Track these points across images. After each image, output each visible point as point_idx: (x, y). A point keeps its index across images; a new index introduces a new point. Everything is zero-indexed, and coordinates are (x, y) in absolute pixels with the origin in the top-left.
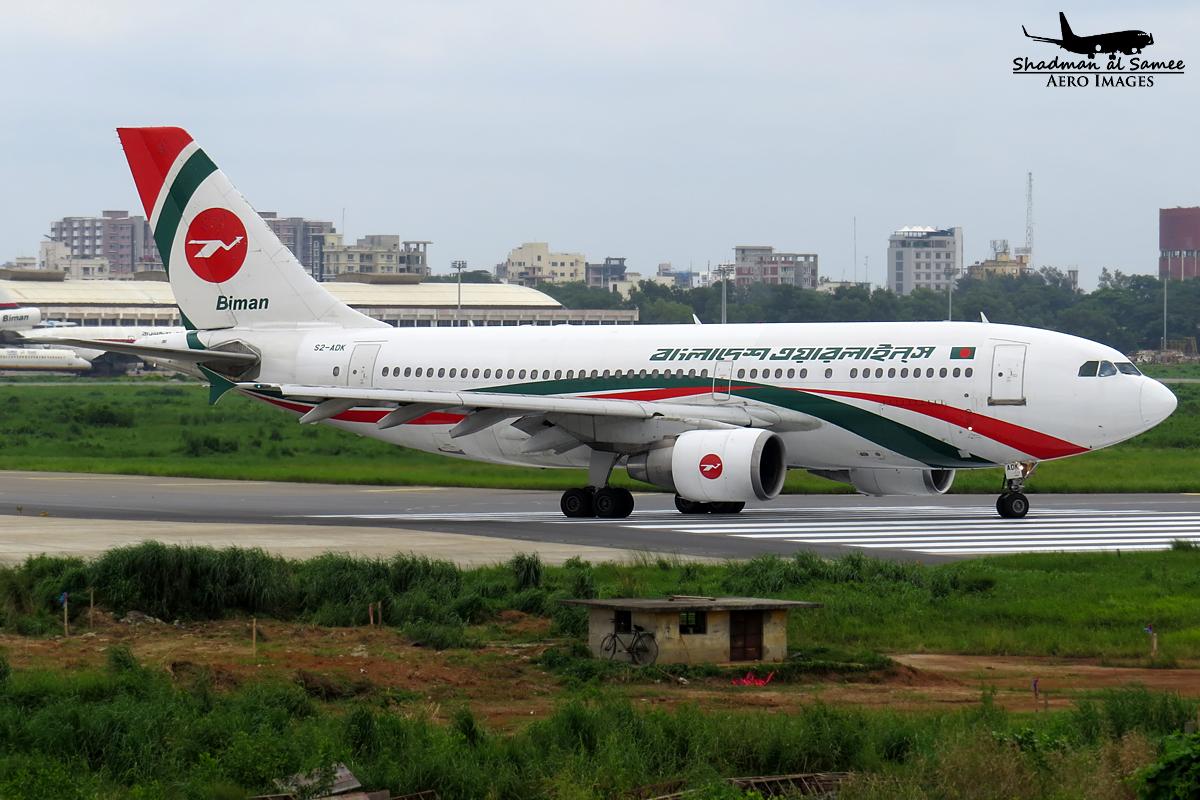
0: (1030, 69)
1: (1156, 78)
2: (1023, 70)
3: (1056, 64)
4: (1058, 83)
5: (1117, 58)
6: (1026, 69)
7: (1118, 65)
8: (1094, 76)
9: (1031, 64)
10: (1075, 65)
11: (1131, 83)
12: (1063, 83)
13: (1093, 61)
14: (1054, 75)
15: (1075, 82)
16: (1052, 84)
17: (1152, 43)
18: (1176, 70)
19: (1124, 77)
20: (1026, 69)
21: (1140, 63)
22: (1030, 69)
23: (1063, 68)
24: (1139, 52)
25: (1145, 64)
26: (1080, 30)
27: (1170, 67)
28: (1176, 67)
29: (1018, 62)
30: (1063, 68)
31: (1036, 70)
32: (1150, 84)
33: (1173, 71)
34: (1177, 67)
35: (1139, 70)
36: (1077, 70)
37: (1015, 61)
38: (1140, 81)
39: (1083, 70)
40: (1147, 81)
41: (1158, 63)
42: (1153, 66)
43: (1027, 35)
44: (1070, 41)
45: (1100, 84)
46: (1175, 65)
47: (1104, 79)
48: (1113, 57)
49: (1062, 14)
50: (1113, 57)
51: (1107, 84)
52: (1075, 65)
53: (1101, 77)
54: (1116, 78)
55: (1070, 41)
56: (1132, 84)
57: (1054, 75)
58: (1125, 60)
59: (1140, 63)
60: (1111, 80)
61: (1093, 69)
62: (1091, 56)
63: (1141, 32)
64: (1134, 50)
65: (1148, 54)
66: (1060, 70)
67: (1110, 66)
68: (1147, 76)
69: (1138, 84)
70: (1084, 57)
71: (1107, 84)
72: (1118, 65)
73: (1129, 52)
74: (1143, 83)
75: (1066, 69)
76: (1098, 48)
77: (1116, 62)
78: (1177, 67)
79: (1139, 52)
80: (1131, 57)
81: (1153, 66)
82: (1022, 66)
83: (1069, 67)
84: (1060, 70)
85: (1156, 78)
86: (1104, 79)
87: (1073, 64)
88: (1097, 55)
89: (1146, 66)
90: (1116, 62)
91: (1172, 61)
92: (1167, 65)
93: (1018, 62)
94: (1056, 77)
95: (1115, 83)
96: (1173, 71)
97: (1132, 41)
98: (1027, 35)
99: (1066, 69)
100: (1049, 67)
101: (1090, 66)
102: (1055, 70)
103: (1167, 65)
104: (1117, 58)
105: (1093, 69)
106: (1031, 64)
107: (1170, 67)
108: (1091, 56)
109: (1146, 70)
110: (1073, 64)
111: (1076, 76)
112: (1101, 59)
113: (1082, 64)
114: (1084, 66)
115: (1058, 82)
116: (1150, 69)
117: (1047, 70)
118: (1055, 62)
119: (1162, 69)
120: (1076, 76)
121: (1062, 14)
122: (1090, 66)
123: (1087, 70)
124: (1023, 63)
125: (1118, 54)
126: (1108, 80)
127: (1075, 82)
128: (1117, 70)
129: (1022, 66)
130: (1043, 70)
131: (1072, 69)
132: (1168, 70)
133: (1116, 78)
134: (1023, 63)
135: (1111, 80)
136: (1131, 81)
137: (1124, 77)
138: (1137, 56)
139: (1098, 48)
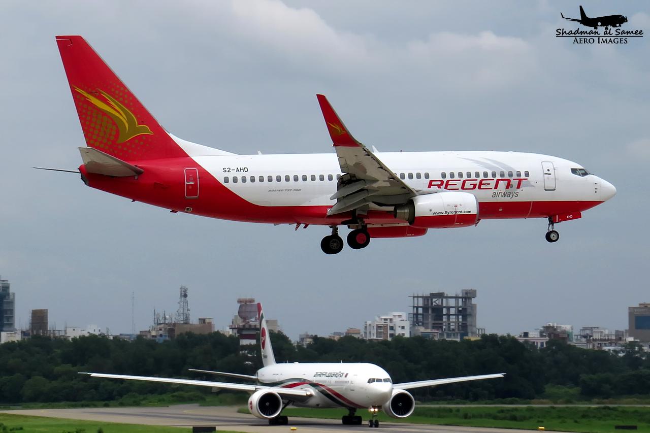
0: (565, 35)
1: (629, 39)
2: (561, 35)
3: (578, 32)
4: (579, 42)
5: (609, 29)
6: (563, 34)
7: (609, 32)
8: (597, 38)
9: (565, 32)
10: (588, 32)
11: (616, 42)
12: (581, 42)
13: (596, 30)
14: (577, 38)
15: (588, 41)
16: (576, 42)
17: (627, 21)
18: (639, 35)
19: (612, 39)
20: (563, 34)
21: (620, 32)
22: (565, 35)
23: (581, 34)
24: (620, 26)
25: (623, 32)
26: (590, 15)
27: (636, 33)
28: (639, 33)
29: (559, 31)
30: (581, 34)
31: (568, 35)
32: (626, 42)
33: (638, 35)
34: (640, 33)
35: (620, 35)
36: (588, 35)
37: (557, 31)
38: (621, 41)
39: (592, 35)
40: (624, 41)
41: (629, 32)
42: (627, 33)
43: (563, 17)
44: (585, 20)
45: (600, 42)
46: (638, 32)
47: (602, 40)
48: (607, 29)
49: (581, 7)
50: (607, 29)
51: (604, 42)
52: (588, 32)
53: (601, 38)
54: (608, 39)
55: (585, 20)
56: (616, 42)
57: (577, 38)
58: (613, 30)
59: (620, 32)
60: (606, 40)
61: (597, 35)
62: (596, 28)
63: (621, 16)
64: (618, 25)
65: (624, 27)
66: (580, 35)
67: (605, 33)
68: (624, 38)
69: (619, 42)
70: (592, 29)
71: (604, 42)
72: (609, 32)
73: (614, 26)
74: (622, 42)
75: (583, 35)
76: (599, 24)
77: (608, 31)
78: (640, 33)
79: (620, 26)
80: (617, 28)
81: (627, 33)
82: (561, 33)
83: (584, 34)
84: (580, 35)
85: (629, 39)
86: (602, 40)
87: (586, 32)
88: (599, 28)
89: (624, 33)
90: (608, 31)
91: (637, 31)
92: (634, 32)
93: (559, 31)
94: (578, 39)
95: (608, 42)
96: (638, 35)
97: (616, 20)
98: (563, 17)
99: (583, 35)
100: (574, 33)
101: (595, 33)
102: (577, 35)
103: (634, 32)
104: (609, 29)
105: (597, 35)
106: (565, 32)
107: (636, 33)
108: (596, 28)
109: (624, 35)
110: (586, 32)
111: (588, 38)
112: (601, 30)
113: (591, 32)
114: (592, 33)
115: (579, 42)
116: (626, 35)
117: (573, 35)
118: (578, 31)
119: (632, 35)
120: (588, 38)
121: (581, 7)
122: (595, 33)
123: (594, 35)
124: (561, 32)
125: (609, 27)
126: (604, 40)
127: (588, 41)
128: (609, 35)
129: (561, 33)
130: (571, 35)
131: (586, 35)
132: (635, 35)
133: (608, 39)
134: (561, 32)
135: (606, 40)
136: (616, 41)
137: (612, 39)
138: (619, 28)
139: (599, 24)
